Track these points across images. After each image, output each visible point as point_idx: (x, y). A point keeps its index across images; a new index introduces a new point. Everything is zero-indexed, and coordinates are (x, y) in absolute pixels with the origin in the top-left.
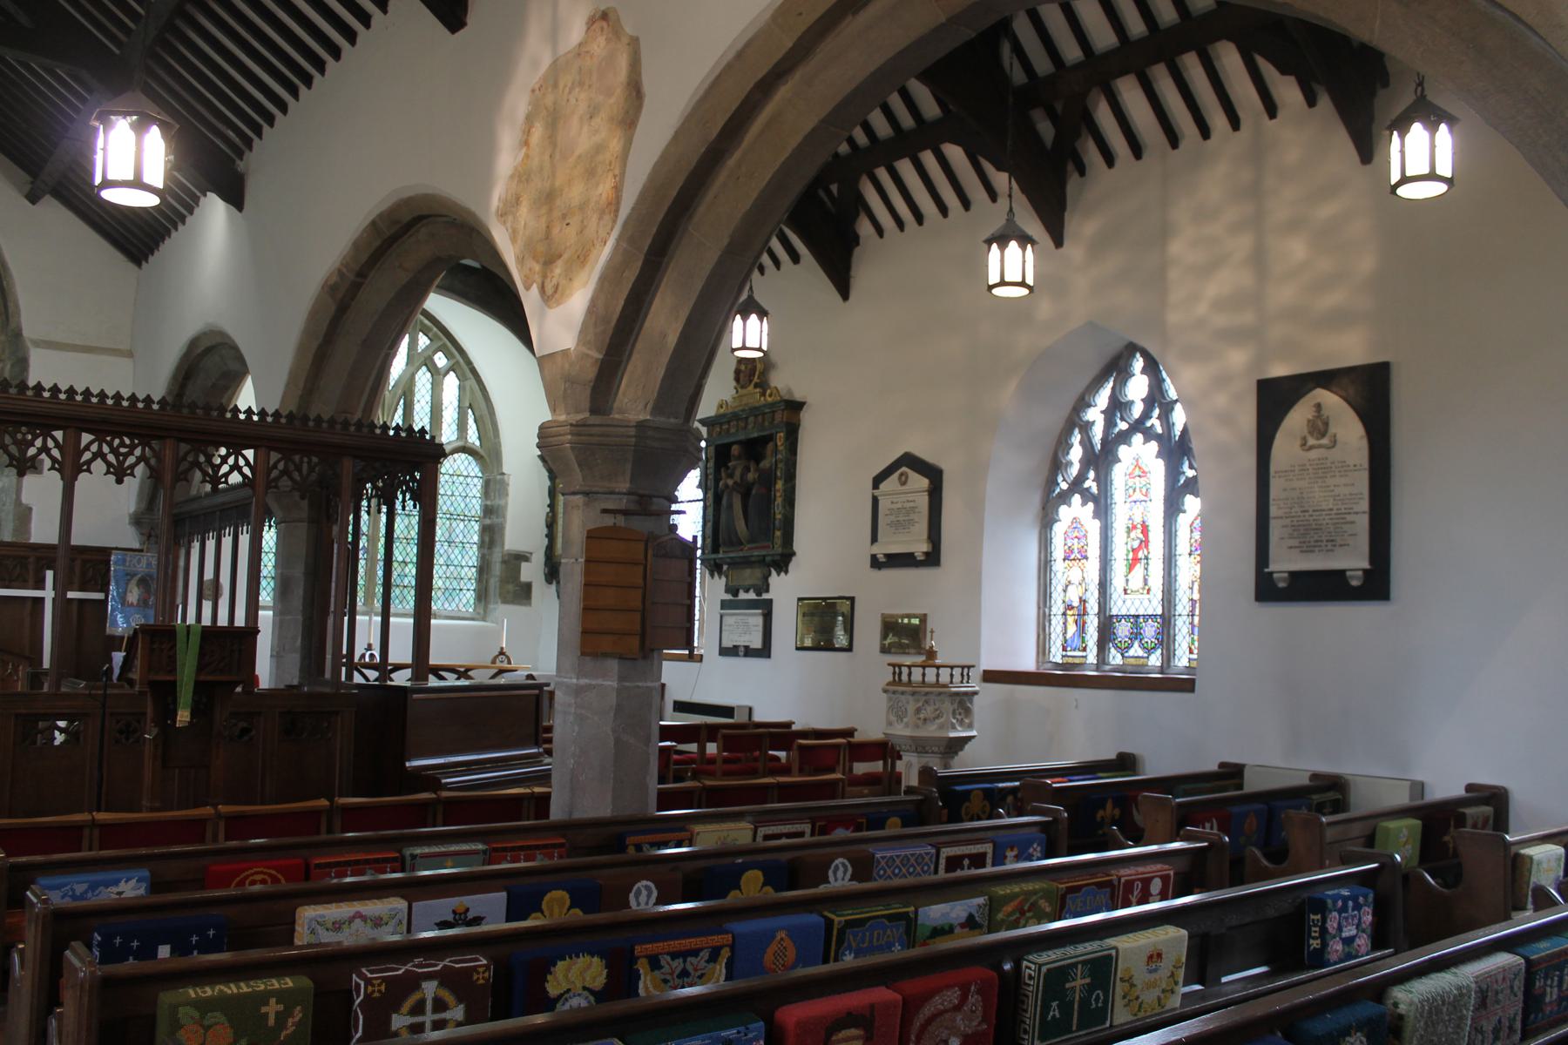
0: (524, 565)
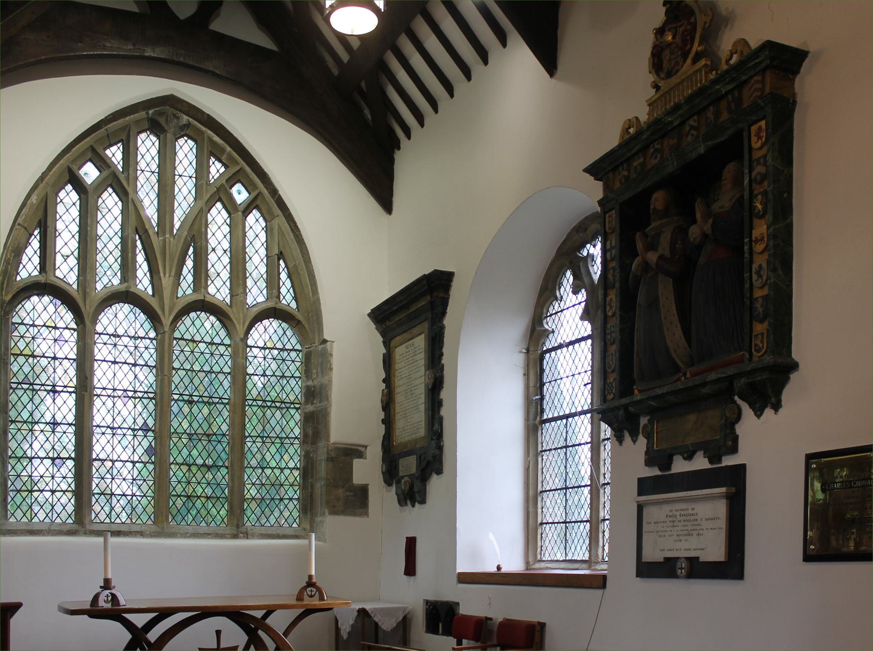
0: (357, 463)
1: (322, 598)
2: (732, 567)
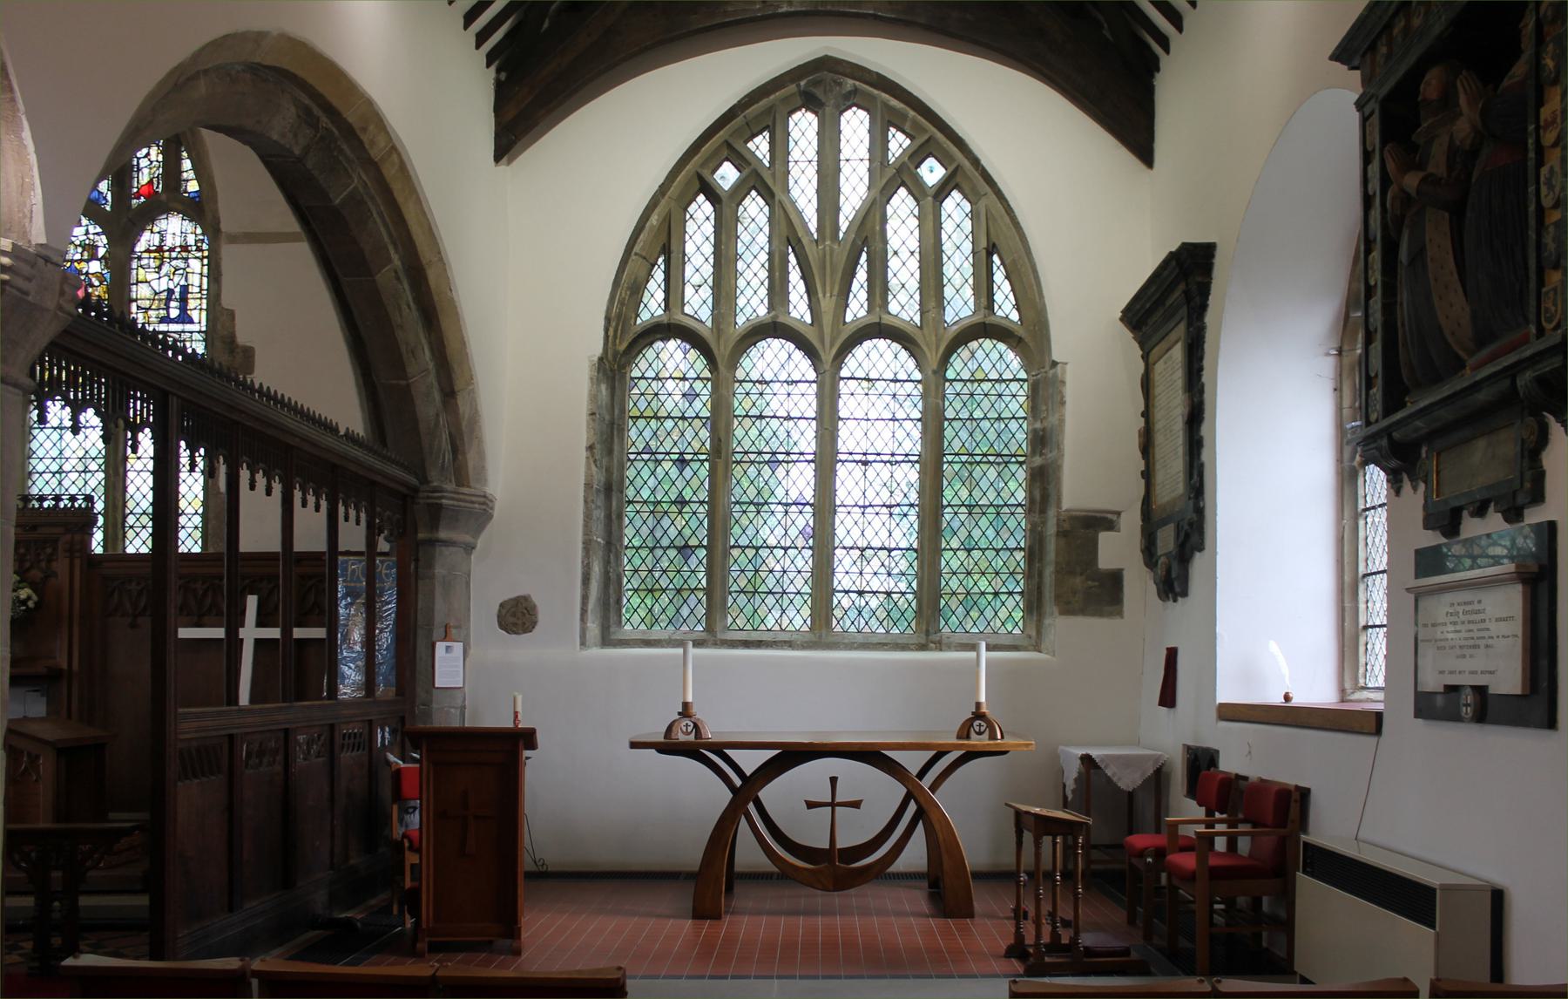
0: (1104, 538)
1: (993, 736)
2: (1536, 704)
